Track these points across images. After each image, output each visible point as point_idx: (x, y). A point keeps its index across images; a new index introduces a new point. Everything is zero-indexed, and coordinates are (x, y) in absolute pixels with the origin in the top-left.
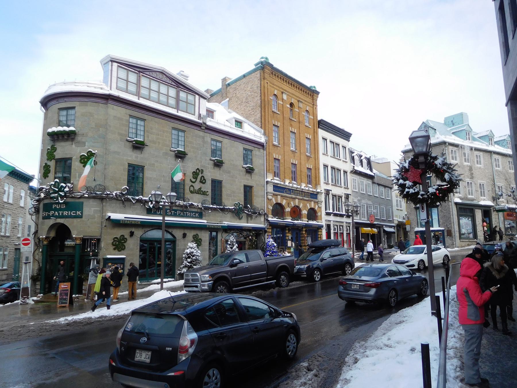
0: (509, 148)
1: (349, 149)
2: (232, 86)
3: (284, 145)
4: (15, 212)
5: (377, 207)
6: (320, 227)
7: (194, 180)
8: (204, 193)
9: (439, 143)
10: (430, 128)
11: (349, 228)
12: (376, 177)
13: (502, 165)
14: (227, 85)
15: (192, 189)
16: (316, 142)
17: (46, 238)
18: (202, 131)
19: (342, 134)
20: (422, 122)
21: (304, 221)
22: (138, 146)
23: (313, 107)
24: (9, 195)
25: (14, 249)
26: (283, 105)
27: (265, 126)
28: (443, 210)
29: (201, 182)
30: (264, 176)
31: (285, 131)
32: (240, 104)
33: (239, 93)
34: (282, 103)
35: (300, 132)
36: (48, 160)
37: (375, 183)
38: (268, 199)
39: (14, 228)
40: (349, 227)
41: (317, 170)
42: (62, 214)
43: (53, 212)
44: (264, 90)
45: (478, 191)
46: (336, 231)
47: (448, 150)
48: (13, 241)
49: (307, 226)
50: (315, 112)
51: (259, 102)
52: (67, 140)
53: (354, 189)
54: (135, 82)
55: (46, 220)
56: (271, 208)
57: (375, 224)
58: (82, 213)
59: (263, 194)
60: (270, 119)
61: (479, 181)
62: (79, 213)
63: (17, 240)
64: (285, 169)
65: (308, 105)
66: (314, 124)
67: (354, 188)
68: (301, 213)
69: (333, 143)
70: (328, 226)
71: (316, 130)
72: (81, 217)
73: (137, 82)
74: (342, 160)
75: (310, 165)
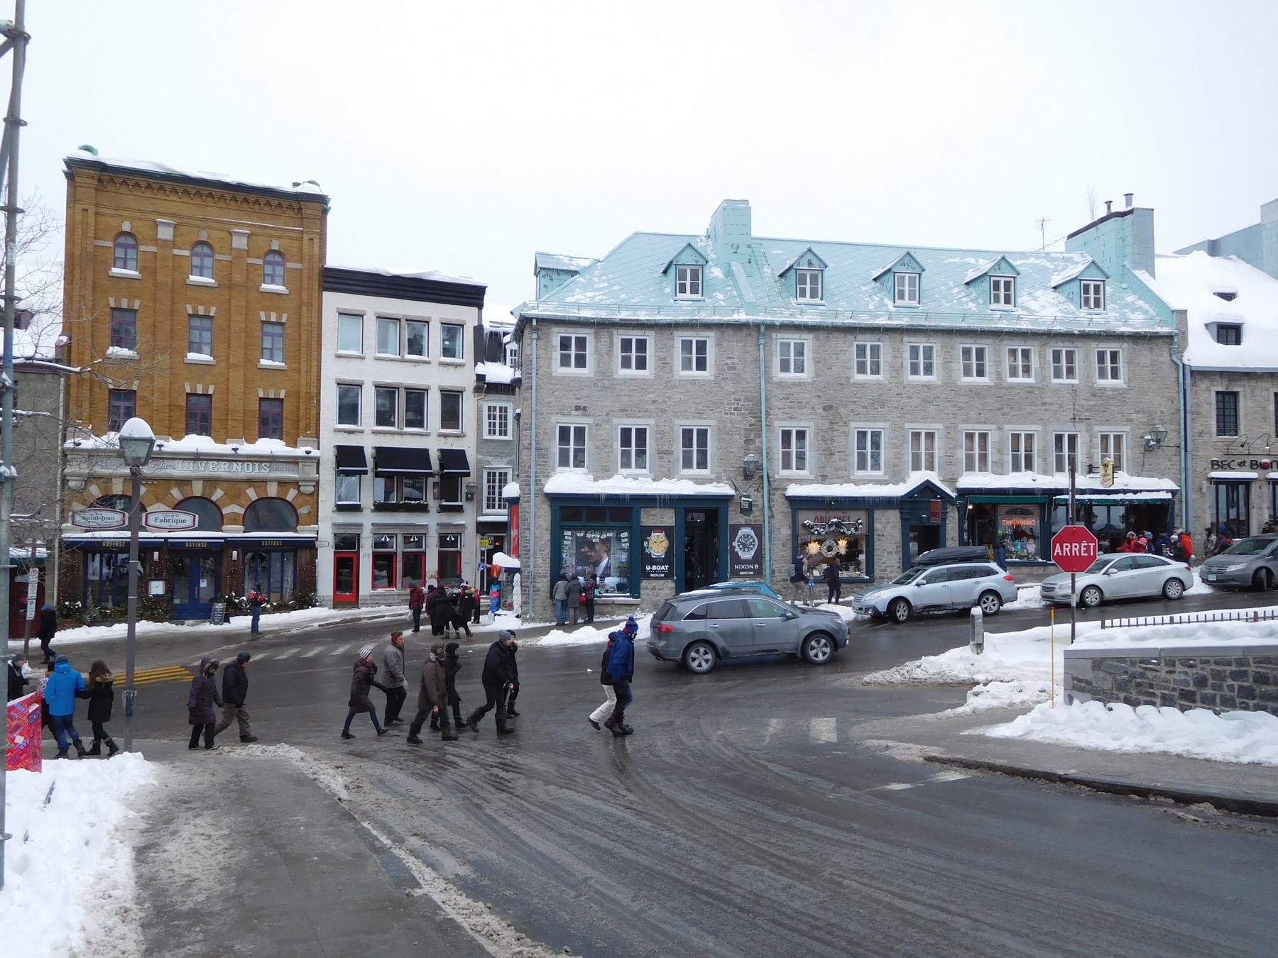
6: (310, 546)
13: (817, 361)
45: (670, 453)
53: (493, 432)
61: (681, 424)
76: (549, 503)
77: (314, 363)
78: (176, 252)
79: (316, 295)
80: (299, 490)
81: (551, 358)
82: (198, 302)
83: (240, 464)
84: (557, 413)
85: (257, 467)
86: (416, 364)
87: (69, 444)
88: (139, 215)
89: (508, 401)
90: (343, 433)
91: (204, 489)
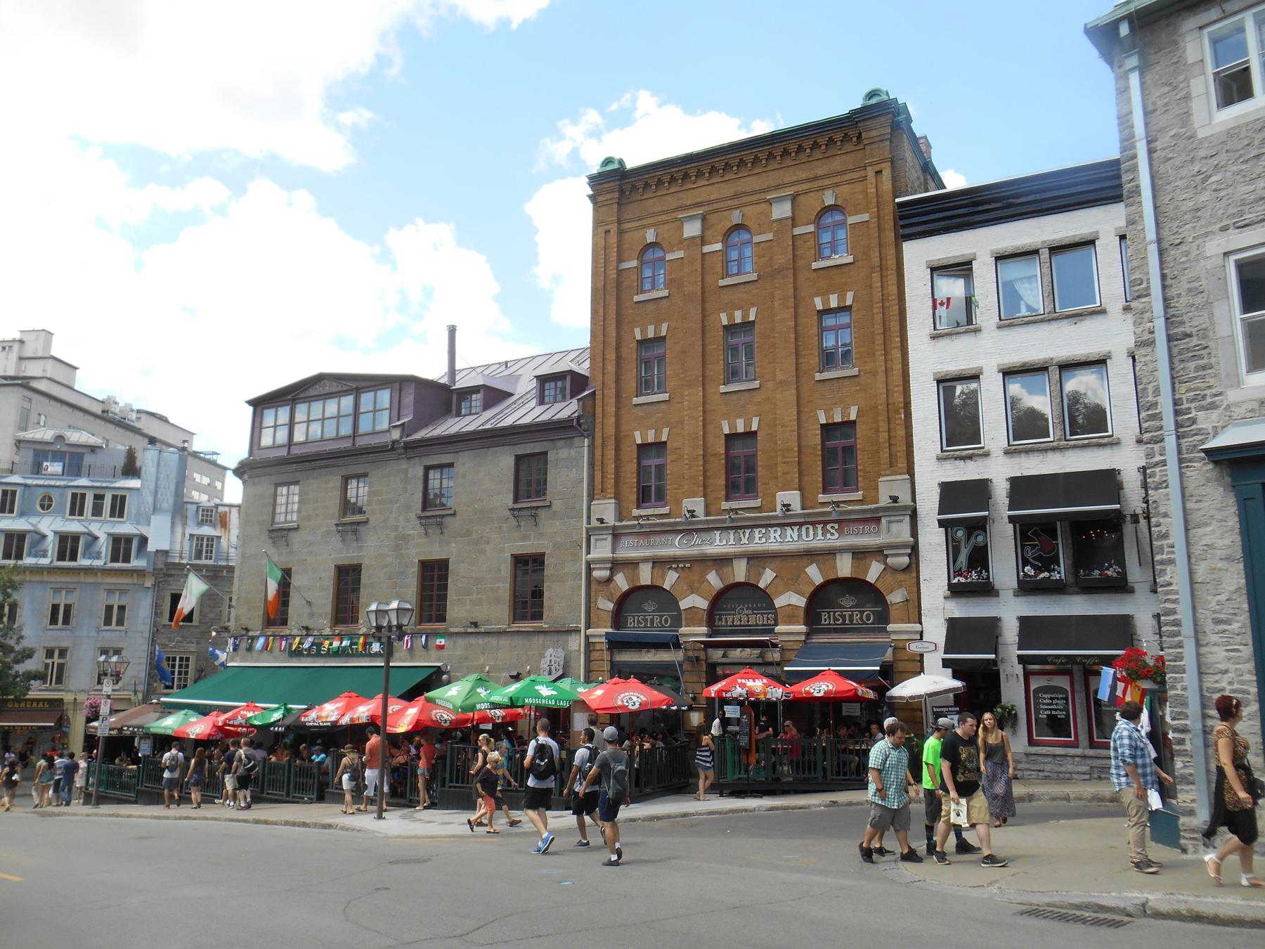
18: (402, 459)
56: (610, 606)
76: (1228, 479)
77: (897, 354)
78: (707, 249)
79: (892, 252)
80: (886, 564)
81: (1187, 97)
82: (730, 307)
83: (796, 528)
84: (1224, 229)
85: (820, 532)
86: (1075, 320)
88: (664, 217)
90: (952, 461)
91: (748, 571)
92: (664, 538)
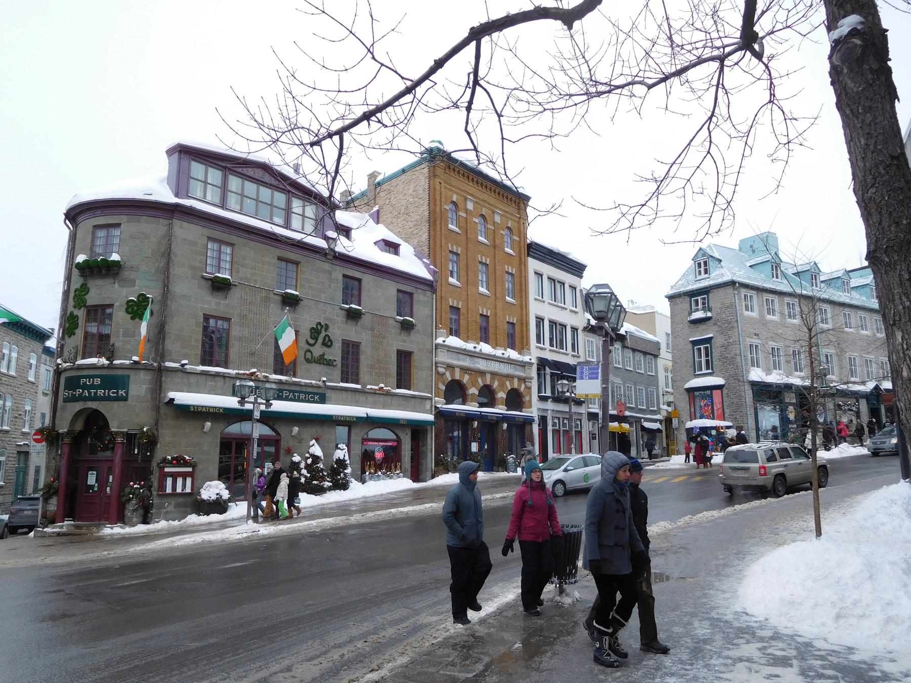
0: (845, 292)
1: (581, 291)
2: (384, 187)
3: (467, 285)
4: (19, 390)
5: (631, 387)
6: (529, 421)
7: (312, 342)
8: (330, 363)
9: (724, 284)
10: (710, 259)
11: (579, 423)
12: (628, 337)
14: (376, 185)
15: (309, 355)
16: (523, 279)
17: (69, 433)
18: (328, 262)
19: (570, 267)
20: (699, 249)
21: (500, 410)
22: (220, 286)
23: (519, 222)
24: (9, 361)
25: (16, 452)
26: (466, 218)
27: (435, 254)
28: (731, 393)
29: (324, 344)
30: (432, 336)
31: (470, 262)
32: (396, 217)
33: (395, 198)
34: (465, 215)
35: (495, 264)
36: (75, 307)
37: (628, 348)
38: (437, 373)
39: (16, 417)
40: (580, 420)
41: (524, 325)
42: (96, 393)
43: (81, 390)
44: (434, 195)
46: (558, 428)
47: (739, 293)
48: (15, 440)
49: (505, 418)
50: (522, 230)
51: (427, 213)
52: (106, 276)
53: (589, 357)
54: (219, 184)
55: (68, 404)
56: (443, 388)
57: (627, 417)
58: (127, 393)
59: (430, 366)
60: (443, 241)
62: (122, 392)
63: (21, 437)
64: (468, 323)
65: (511, 219)
66: (520, 250)
67: (589, 355)
68: (496, 397)
69: (554, 281)
70: (543, 420)
71: (523, 260)
72: (125, 399)
73: (222, 186)
74: (568, 310)
75: (513, 317)
87: (440, 340)
89: (593, 337)
92: (464, 357)
